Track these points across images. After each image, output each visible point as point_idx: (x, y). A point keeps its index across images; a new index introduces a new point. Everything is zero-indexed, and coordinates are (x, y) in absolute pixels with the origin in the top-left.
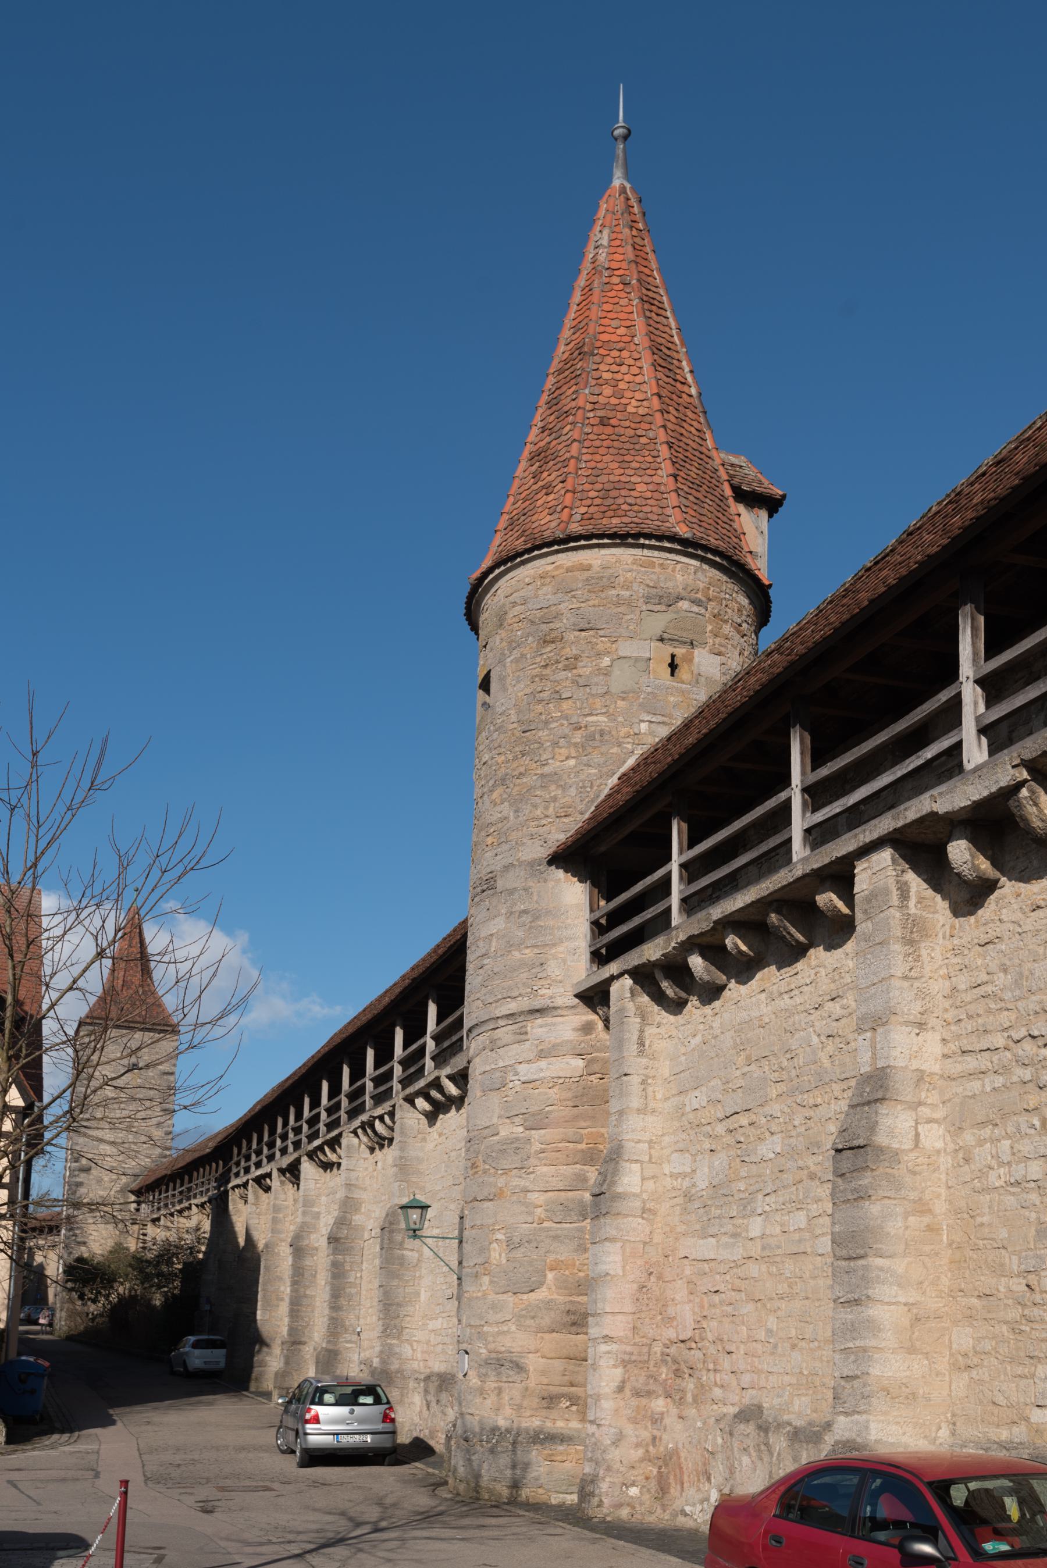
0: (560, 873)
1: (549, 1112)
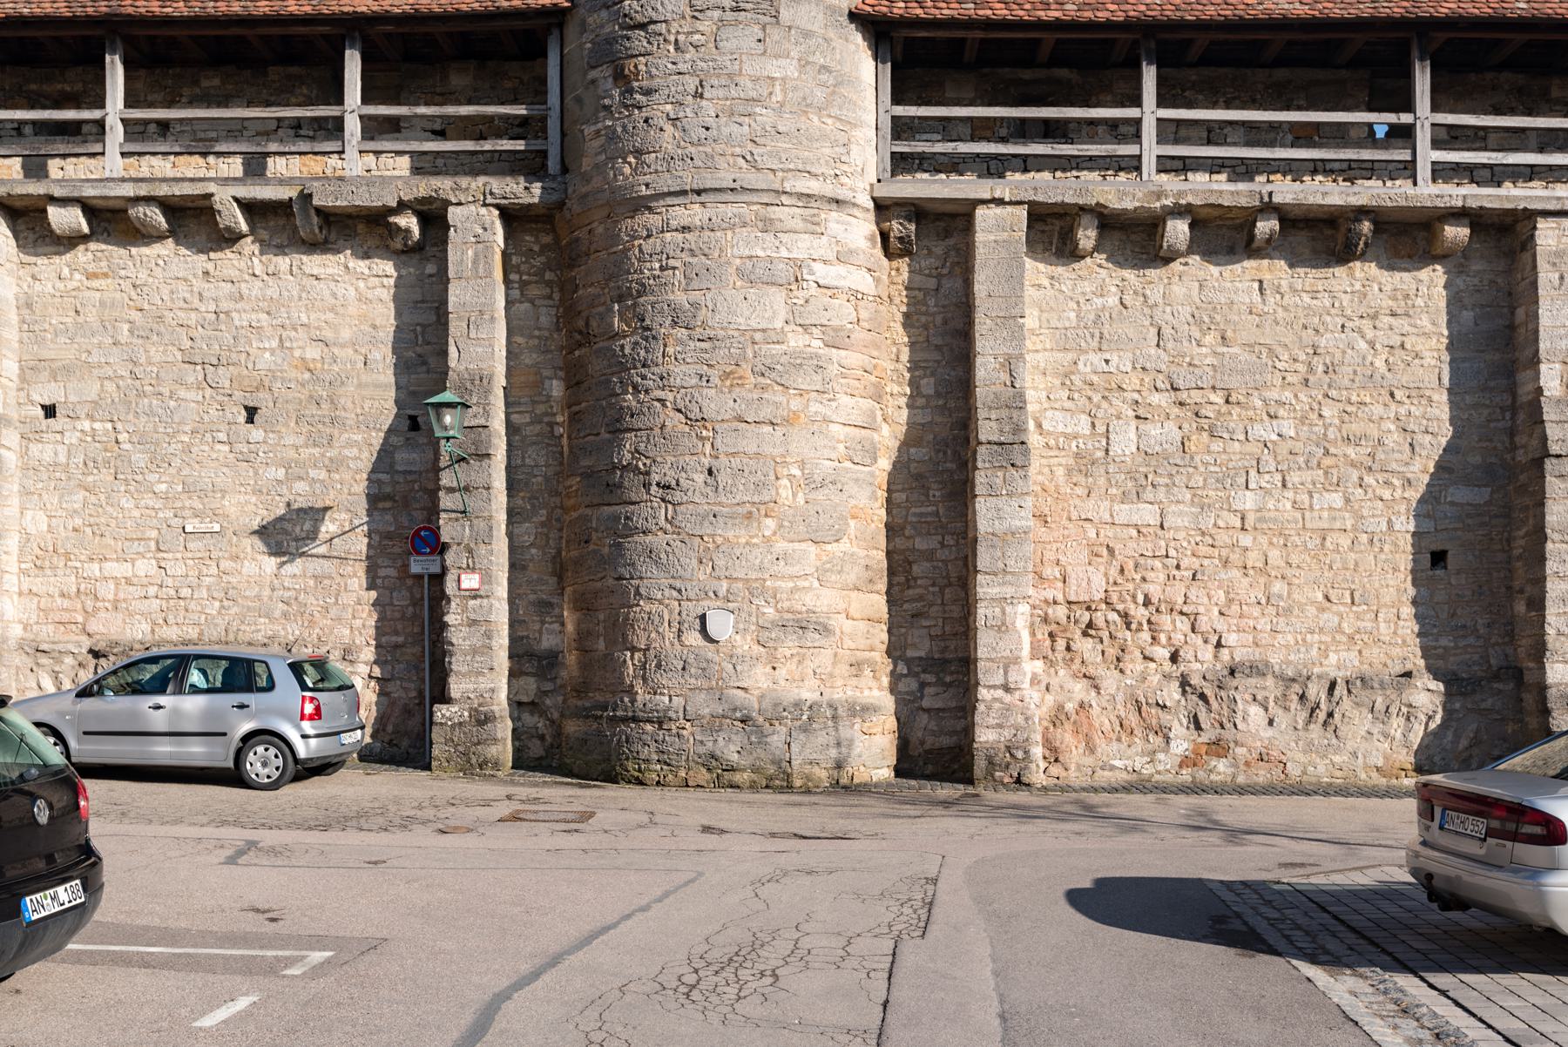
0: (858, 39)
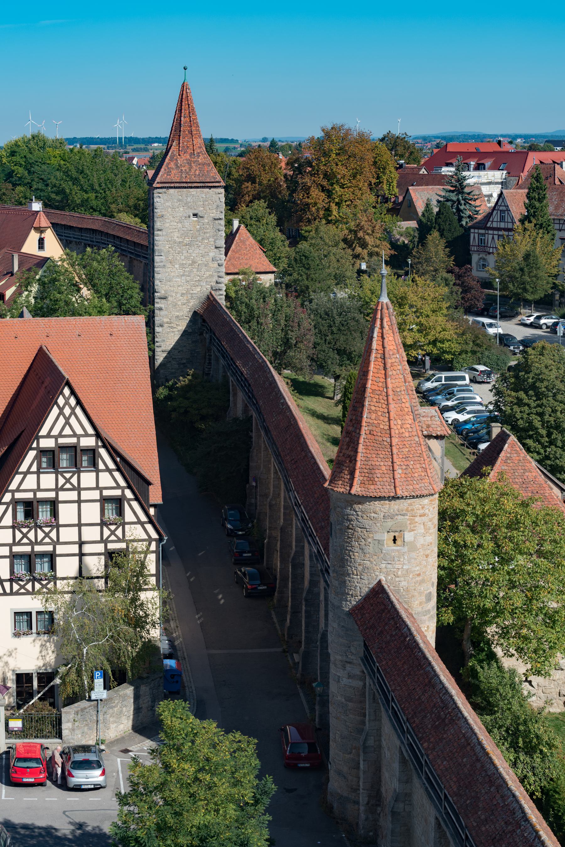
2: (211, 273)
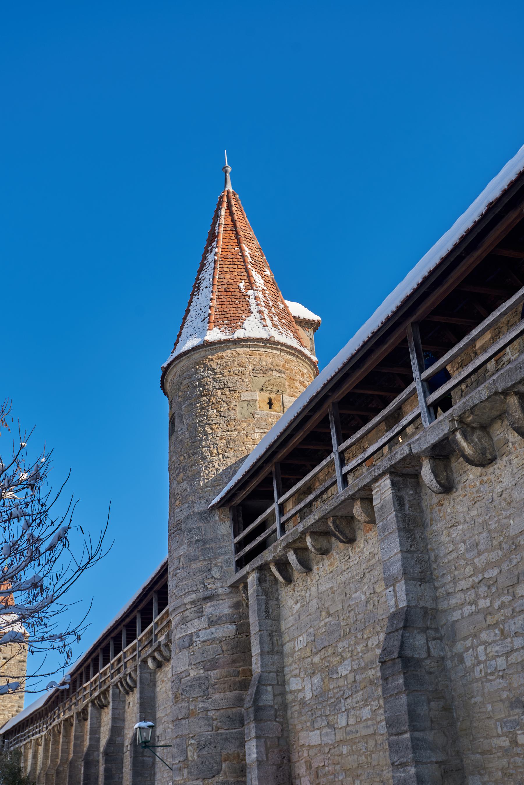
1: (218, 659)
2: (13, 704)
